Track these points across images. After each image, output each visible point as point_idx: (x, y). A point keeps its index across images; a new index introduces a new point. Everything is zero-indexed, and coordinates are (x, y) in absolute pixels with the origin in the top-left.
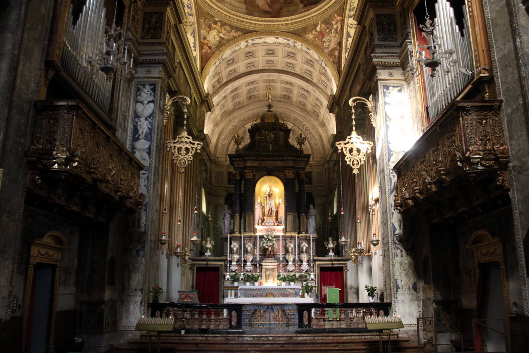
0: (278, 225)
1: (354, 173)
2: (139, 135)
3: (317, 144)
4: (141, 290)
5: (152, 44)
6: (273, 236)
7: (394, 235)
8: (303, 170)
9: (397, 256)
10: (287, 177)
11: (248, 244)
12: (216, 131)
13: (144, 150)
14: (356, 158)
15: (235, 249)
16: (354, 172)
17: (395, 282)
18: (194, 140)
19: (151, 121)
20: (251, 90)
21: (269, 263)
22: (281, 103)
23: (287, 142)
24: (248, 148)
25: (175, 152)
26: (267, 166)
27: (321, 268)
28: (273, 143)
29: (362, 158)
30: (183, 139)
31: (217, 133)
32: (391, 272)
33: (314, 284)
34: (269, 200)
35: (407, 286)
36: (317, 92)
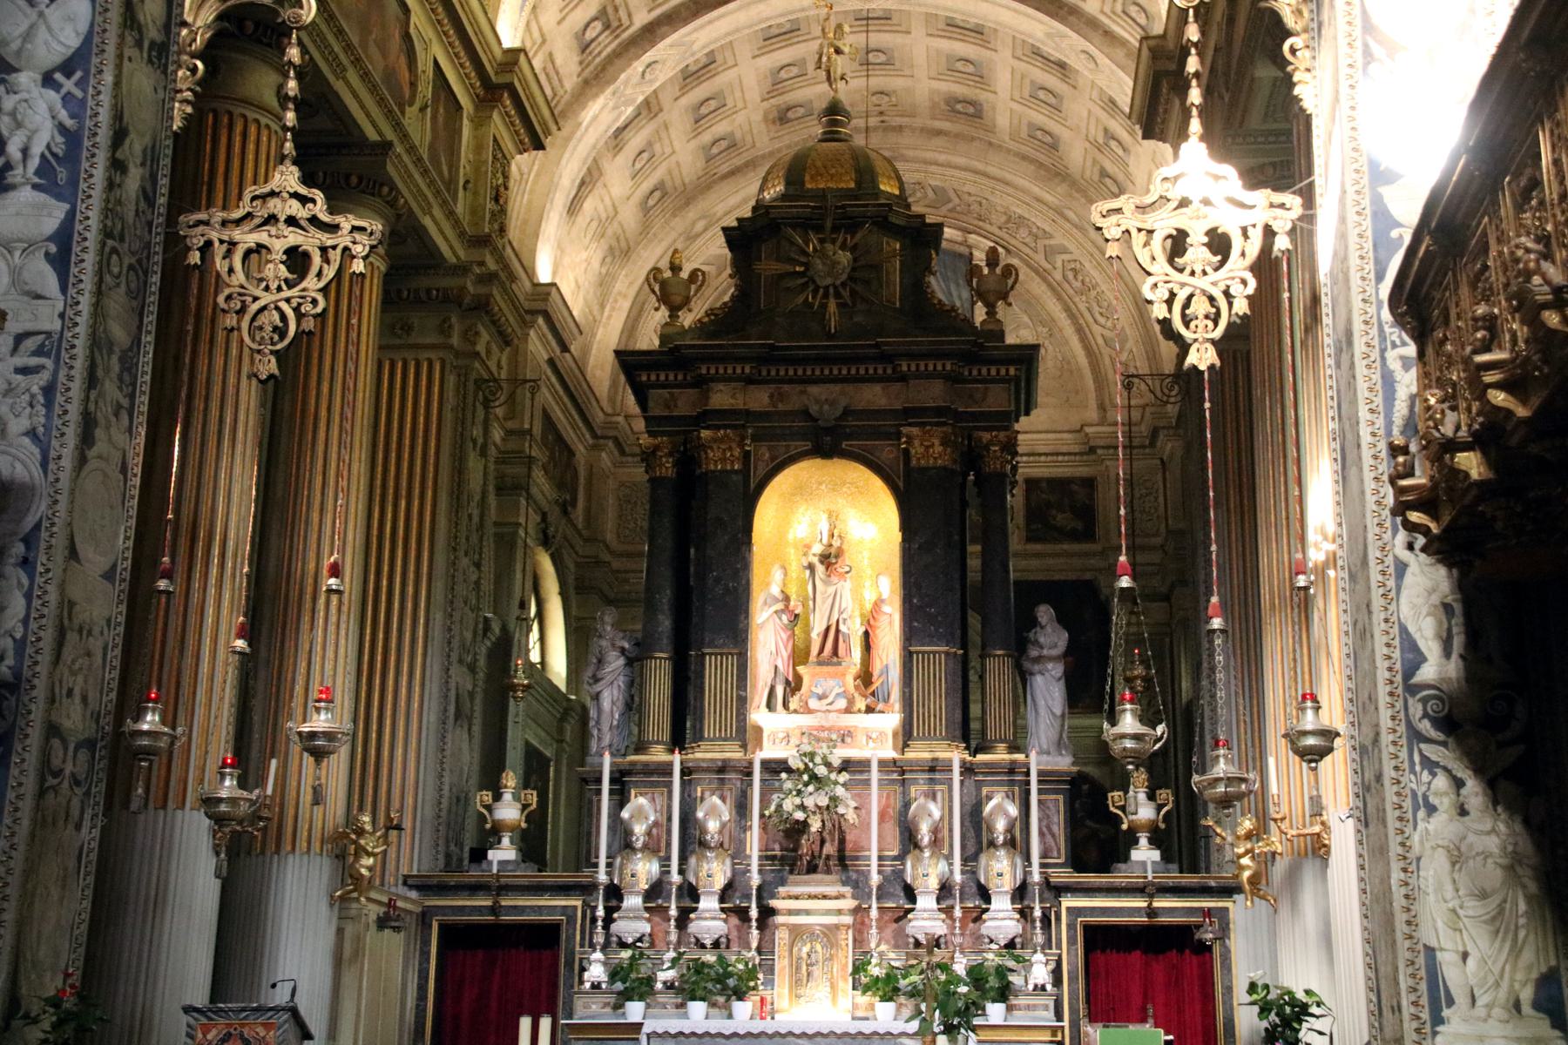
0: (870, 710)
1: (1195, 367)
6: (836, 763)
7: (1411, 689)
8: (998, 429)
9: (1432, 809)
10: (914, 462)
11: (706, 804)
12: (619, 286)
13: (30, 246)
15: (639, 829)
16: (1192, 359)
17: (1421, 961)
18: (332, 211)
19: (79, 94)
20: (783, 74)
21: (811, 897)
22: (939, 142)
23: (917, 289)
24: (722, 322)
25: (231, 271)
27: (1089, 930)
28: (846, 293)
29: (1238, 280)
30: (274, 205)
31: (625, 296)
32: (1399, 901)
33: (1051, 1014)
34: (827, 583)
35: (1502, 994)
36: (1103, 60)
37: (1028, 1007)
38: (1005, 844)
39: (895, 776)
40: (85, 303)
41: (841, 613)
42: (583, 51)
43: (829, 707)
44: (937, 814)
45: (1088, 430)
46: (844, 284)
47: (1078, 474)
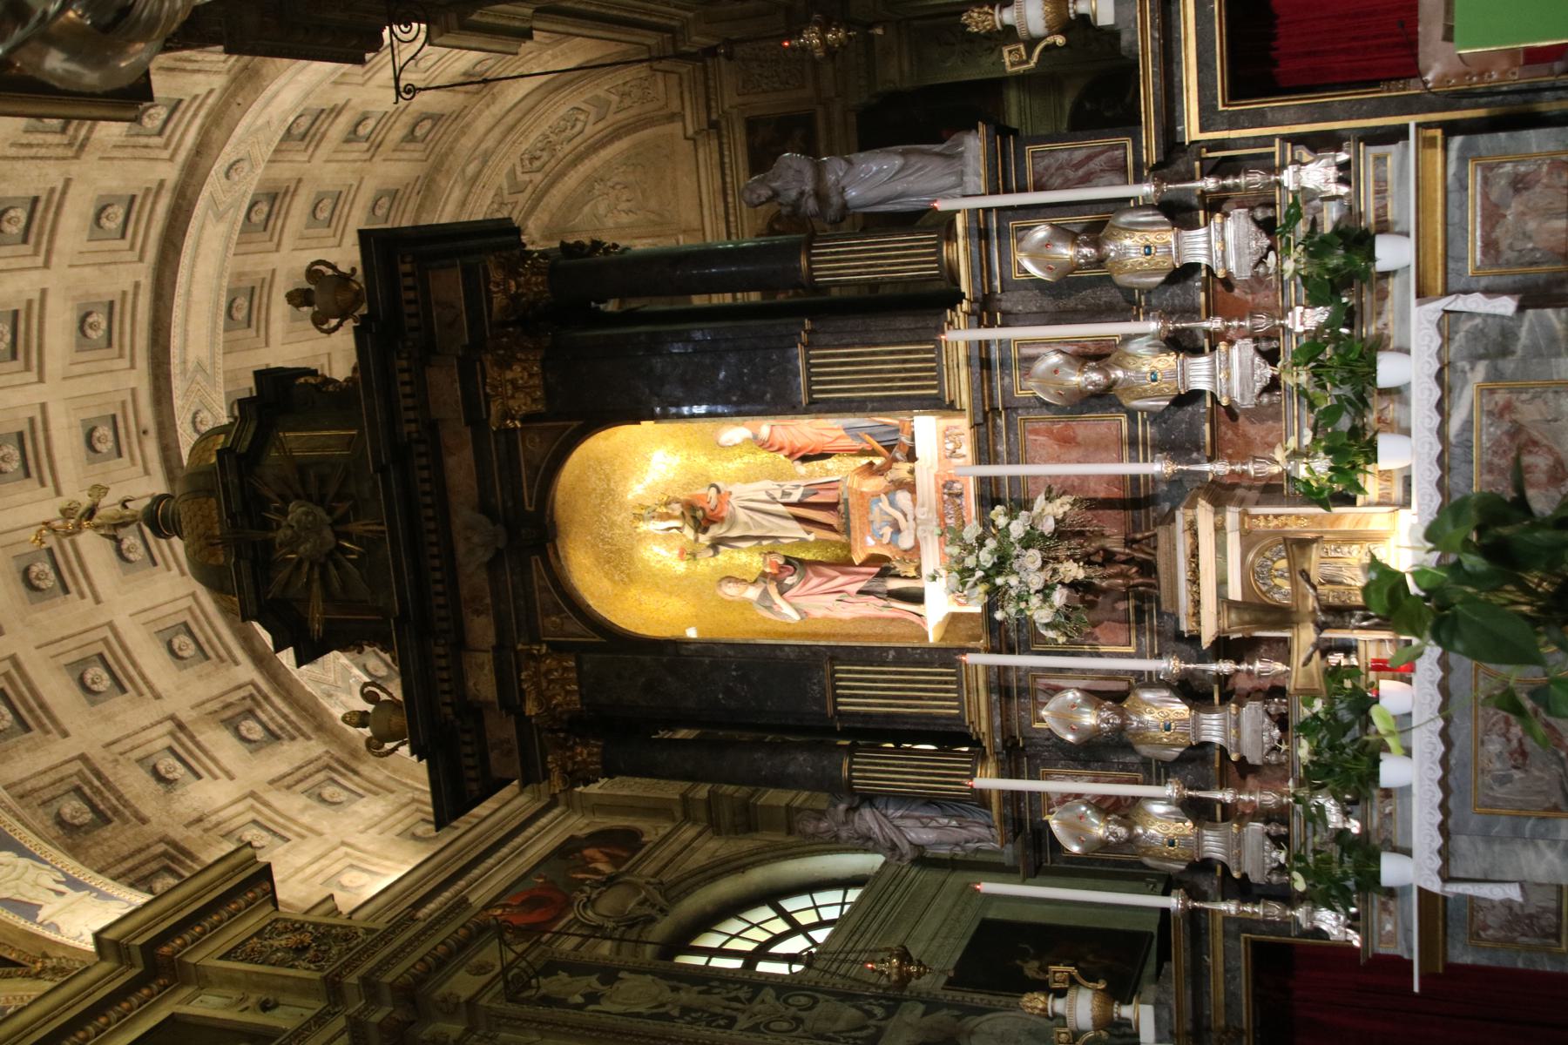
0: (911, 456)
3: (596, 101)
10: (540, 407)
21: (1195, 580)
28: (342, 508)
33: (1392, 151)
34: (733, 523)
37: (1381, 192)
38: (1097, 244)
39: (1002, 422)
41: (774, 501)
42: (278, 738)
43: (910, 517)
44: (1054, 359)
45: (690, 132)
46: (330, 512)
47: (744, 138)
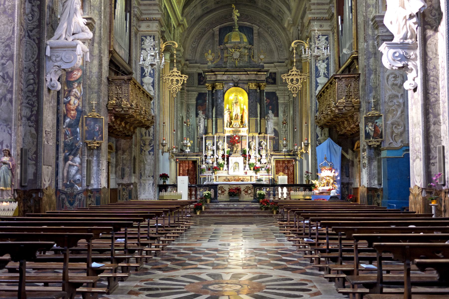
0: (243, 127)
2: (145, 74)
4: (153, 176)
5: (150, 5)
13: (149, 84)
14: (295, 86)
18: (182, 74)
26: (234, 80)
30: (174, 73)
40: (157, 91)
